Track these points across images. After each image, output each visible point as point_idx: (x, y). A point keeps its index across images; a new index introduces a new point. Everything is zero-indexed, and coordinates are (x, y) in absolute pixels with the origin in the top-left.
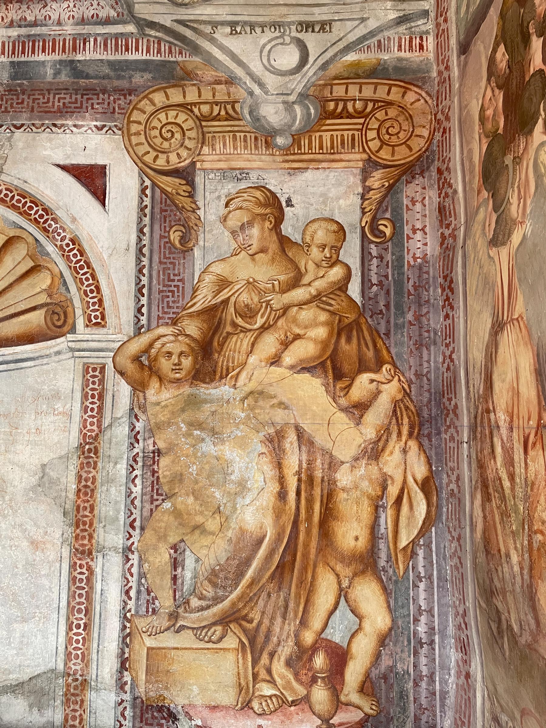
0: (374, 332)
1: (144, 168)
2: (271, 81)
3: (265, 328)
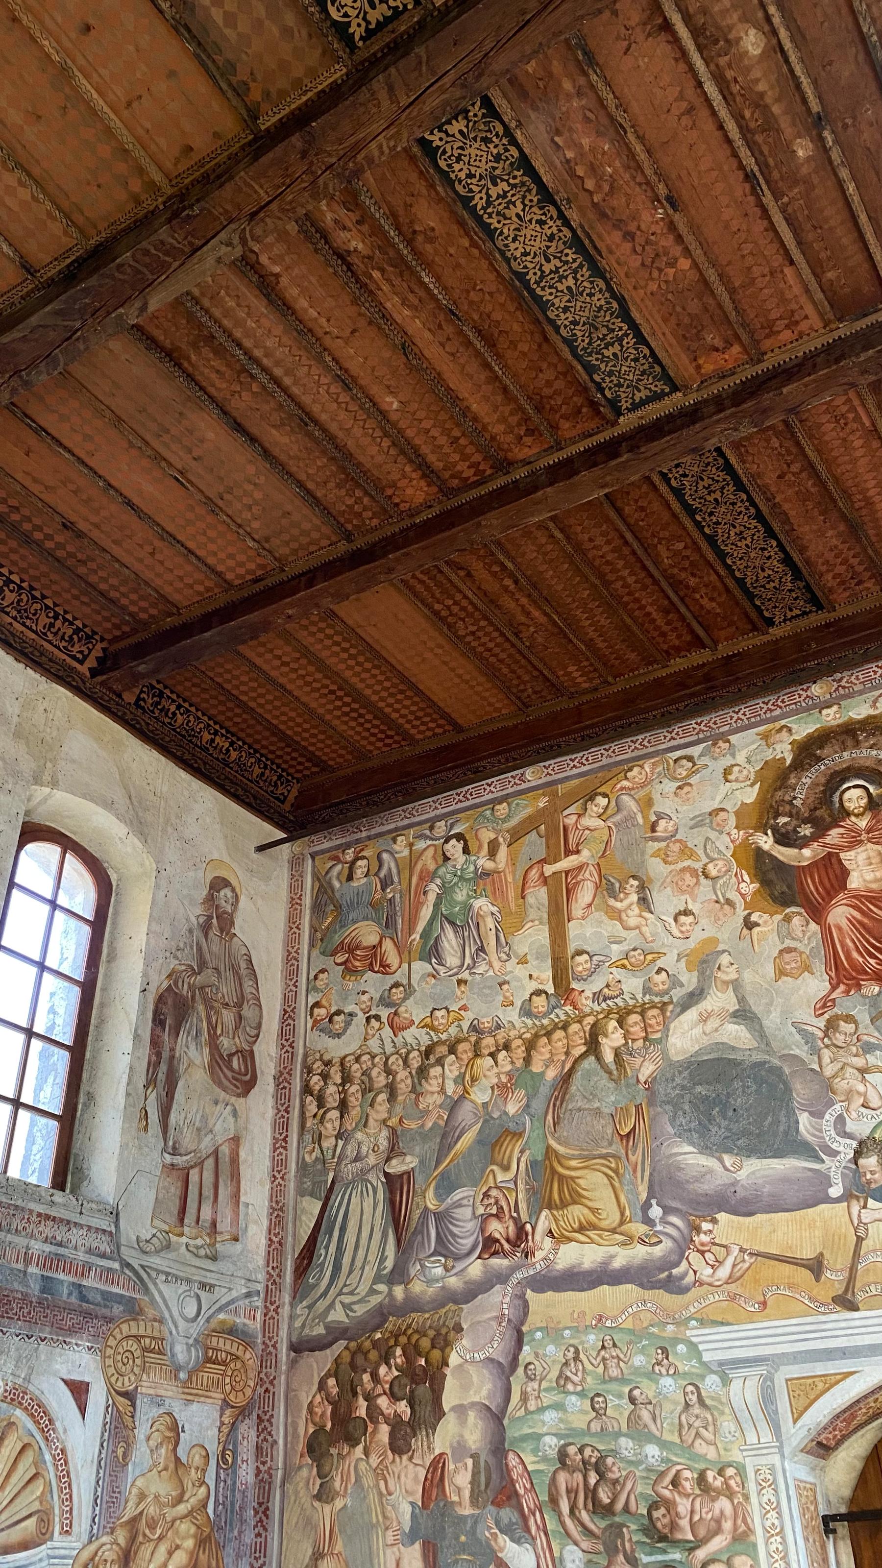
0: (218, 1544)
1: (110, 1386)
2: (181, 1323)
3: (160, 1538)
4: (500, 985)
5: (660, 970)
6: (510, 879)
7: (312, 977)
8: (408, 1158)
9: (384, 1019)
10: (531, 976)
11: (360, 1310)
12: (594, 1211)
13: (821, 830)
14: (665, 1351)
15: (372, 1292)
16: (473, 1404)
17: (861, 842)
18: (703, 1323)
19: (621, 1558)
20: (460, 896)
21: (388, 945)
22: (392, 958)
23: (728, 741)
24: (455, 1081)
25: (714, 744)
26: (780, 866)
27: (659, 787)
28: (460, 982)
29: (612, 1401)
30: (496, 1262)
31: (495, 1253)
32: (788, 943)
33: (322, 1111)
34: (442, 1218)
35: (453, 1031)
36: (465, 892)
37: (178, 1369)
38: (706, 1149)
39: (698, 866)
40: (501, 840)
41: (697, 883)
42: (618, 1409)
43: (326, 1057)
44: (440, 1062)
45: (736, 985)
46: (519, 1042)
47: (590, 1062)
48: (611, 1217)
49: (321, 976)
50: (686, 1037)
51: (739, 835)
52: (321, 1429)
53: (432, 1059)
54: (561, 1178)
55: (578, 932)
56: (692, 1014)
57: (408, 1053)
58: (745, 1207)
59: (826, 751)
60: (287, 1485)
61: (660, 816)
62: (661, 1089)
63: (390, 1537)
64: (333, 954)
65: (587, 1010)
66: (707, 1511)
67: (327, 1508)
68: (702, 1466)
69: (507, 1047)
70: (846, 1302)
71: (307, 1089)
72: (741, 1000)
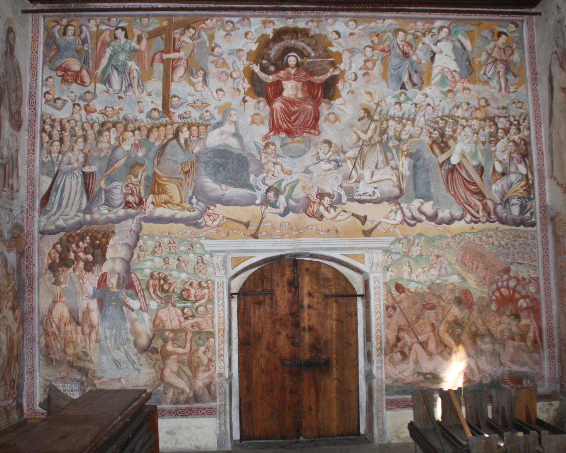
4: (138, 102)
5: (207, 111)
6: (146, 56)
7: (44, 79)
8: (93, 167)
9: (82, 106)
10: (152, 102)
11: (71, 222)
12: (170, 197)
13: (278, 70)
14: (192, 246)
15: (76, 215)
16: (118, 258)
17: (290, 79)
18: (206, 238)
19: (170, 305)
20: (122, 57)
21: (84, 73)
22: (87, 79)
23: (249, 20)
24: (115, 139)
25: (243, 19)
26: (260, 81)
27: (217, 31)
28: (120, 97)
29: (171, 260)
30: (131, 211)
31: (130, 207)
32: (258, 111)
33: (51, 141)
34: (107, 192)
35: (115, 118)
36: (124, 57)
37: (6, 241)
38: (216, 181)
39: (229, 72)
40: (143, 36)
41: (227, 79)
42: (173, 261)
43: (53, 118)
44: (108, 130)
45: (236, 123)
46: (144, 128)
47: (174, 142)
48: (178, 200)
49: (50, 80)
50: (214, 139)
51: (247, 63)
52: (54, 262)
53: (105, 128)
54: (159, 184)
55: (177, 88)
56: (217, 131)
57: (93, 123)
58: (227, 203)
59: (285, 37)
60: (41, 280)
61: (217, 45)
62: (202, 157)
63: (84, 297)
64: (56, 70)
65: (175, 121)
66: (200, 292)
67: (58, 288)
68: (200, 280)
69: (139, 129)
70: (255, 236)
71: (43, 130)
72: (237, 129)
